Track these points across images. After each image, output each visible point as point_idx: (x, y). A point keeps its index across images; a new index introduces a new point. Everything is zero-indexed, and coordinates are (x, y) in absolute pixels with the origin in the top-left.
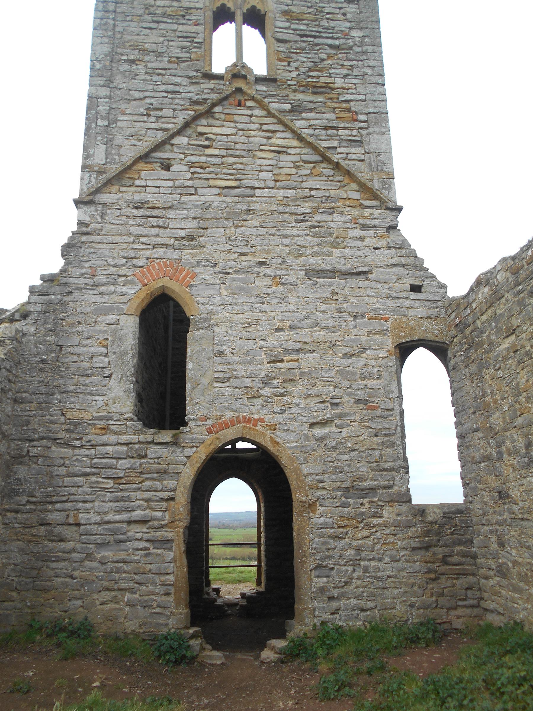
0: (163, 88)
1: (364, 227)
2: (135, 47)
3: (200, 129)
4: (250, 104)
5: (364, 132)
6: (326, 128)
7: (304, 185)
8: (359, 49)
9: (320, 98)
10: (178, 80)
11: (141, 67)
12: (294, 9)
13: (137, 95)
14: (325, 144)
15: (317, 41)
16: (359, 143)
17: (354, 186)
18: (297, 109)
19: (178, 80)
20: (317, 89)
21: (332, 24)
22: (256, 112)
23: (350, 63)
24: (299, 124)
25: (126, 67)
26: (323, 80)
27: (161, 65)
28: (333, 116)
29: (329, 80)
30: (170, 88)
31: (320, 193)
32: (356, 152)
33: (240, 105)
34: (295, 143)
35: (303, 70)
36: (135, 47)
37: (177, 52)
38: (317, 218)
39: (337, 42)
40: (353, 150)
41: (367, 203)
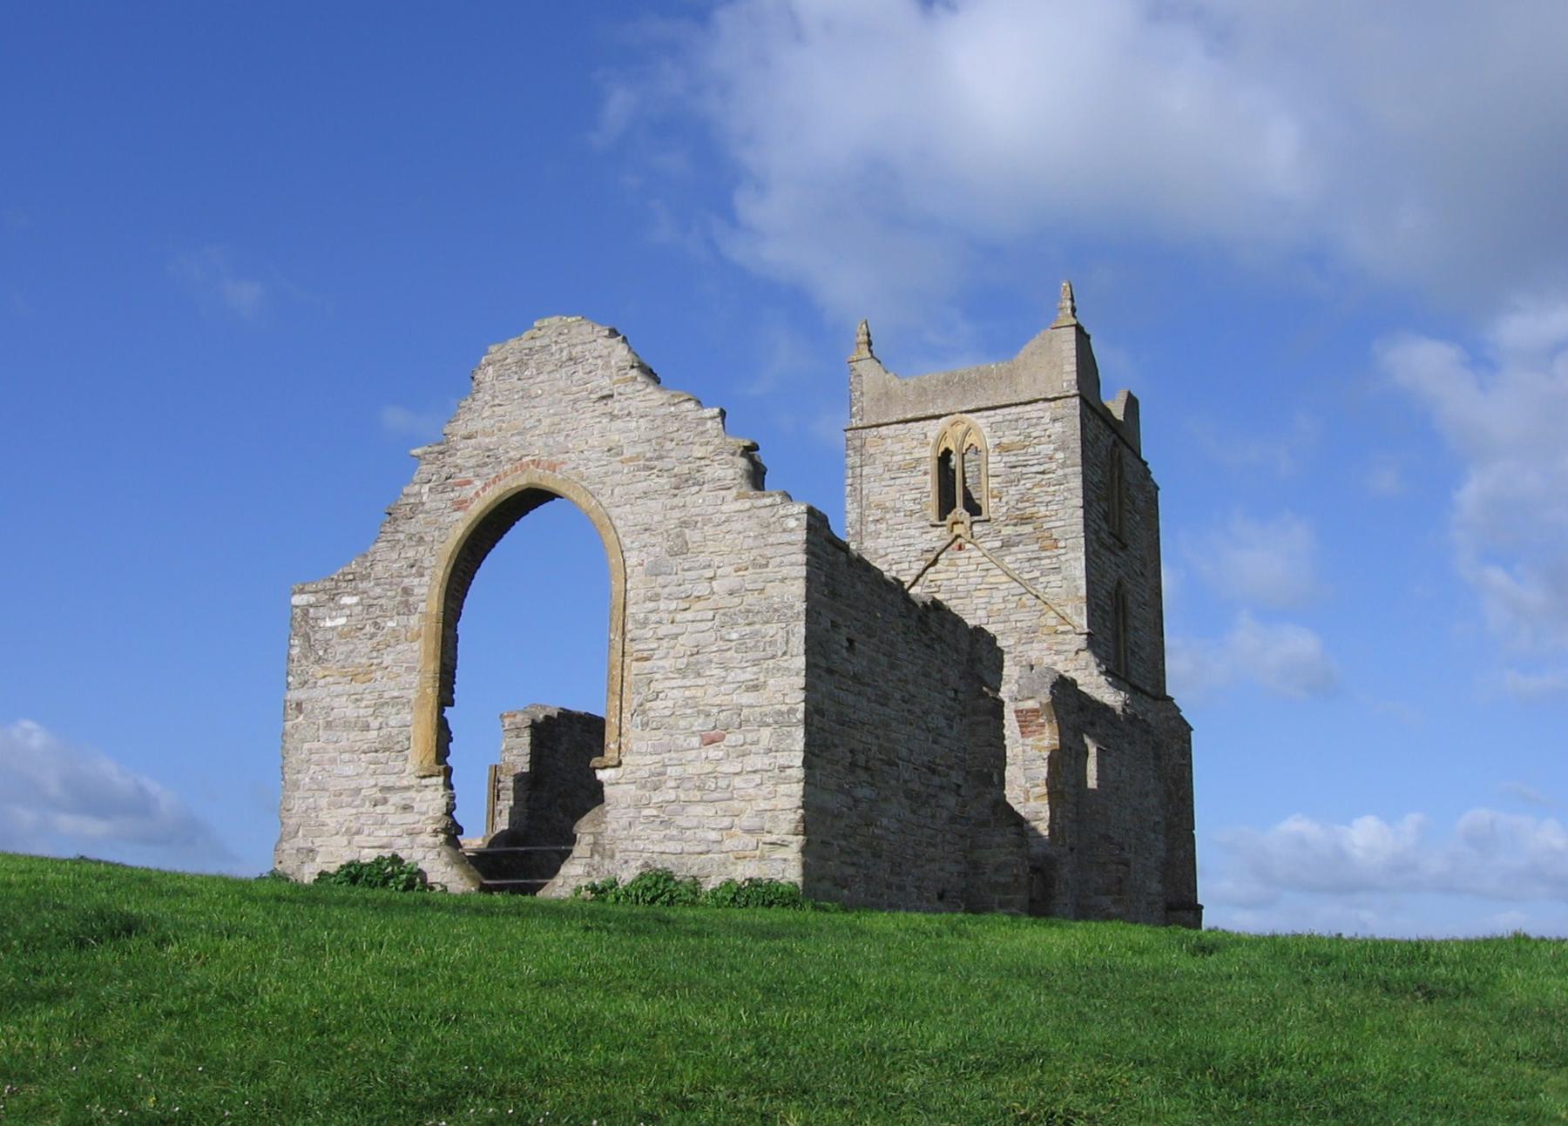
0: (901, 542)
1: (1058, 653)
2: (878, 506)
3: (930, 577)
4: (968, 546)
5: (1063, 558)
6: (1029, 560)
7: (1012, 618)
8: (1060, 472)
9: (1028, 529)
10: (912, 532)
11: (884, 526)
12: (1005, 440)
13: (882, 552)
14: (1026, 576)
15: (1025, 470)
16: (1057, 570)
17: (1052, 614)
18: (1007, 544)
19: (912, 532)
20: (1024, 520)
21: (1038, 448)
22: (974, 554)
23: (1052, 488)
24: (1007, 559)
25: (872, 527)
26: (1028, 511)
27: (898, 520)
28: (1036, 547)
29: (1034, 510)
30: (906, 541)
31: (1024, 624)
32: (1055, 579)
33: (960, 548)
34: (1005, 578)
35: (1012, 503)
36: (878, 506)
37: (911, 506)
38: (1020, 648)
39: (1041, 468)
40: (1052, 578)
41: (1061, 628)
